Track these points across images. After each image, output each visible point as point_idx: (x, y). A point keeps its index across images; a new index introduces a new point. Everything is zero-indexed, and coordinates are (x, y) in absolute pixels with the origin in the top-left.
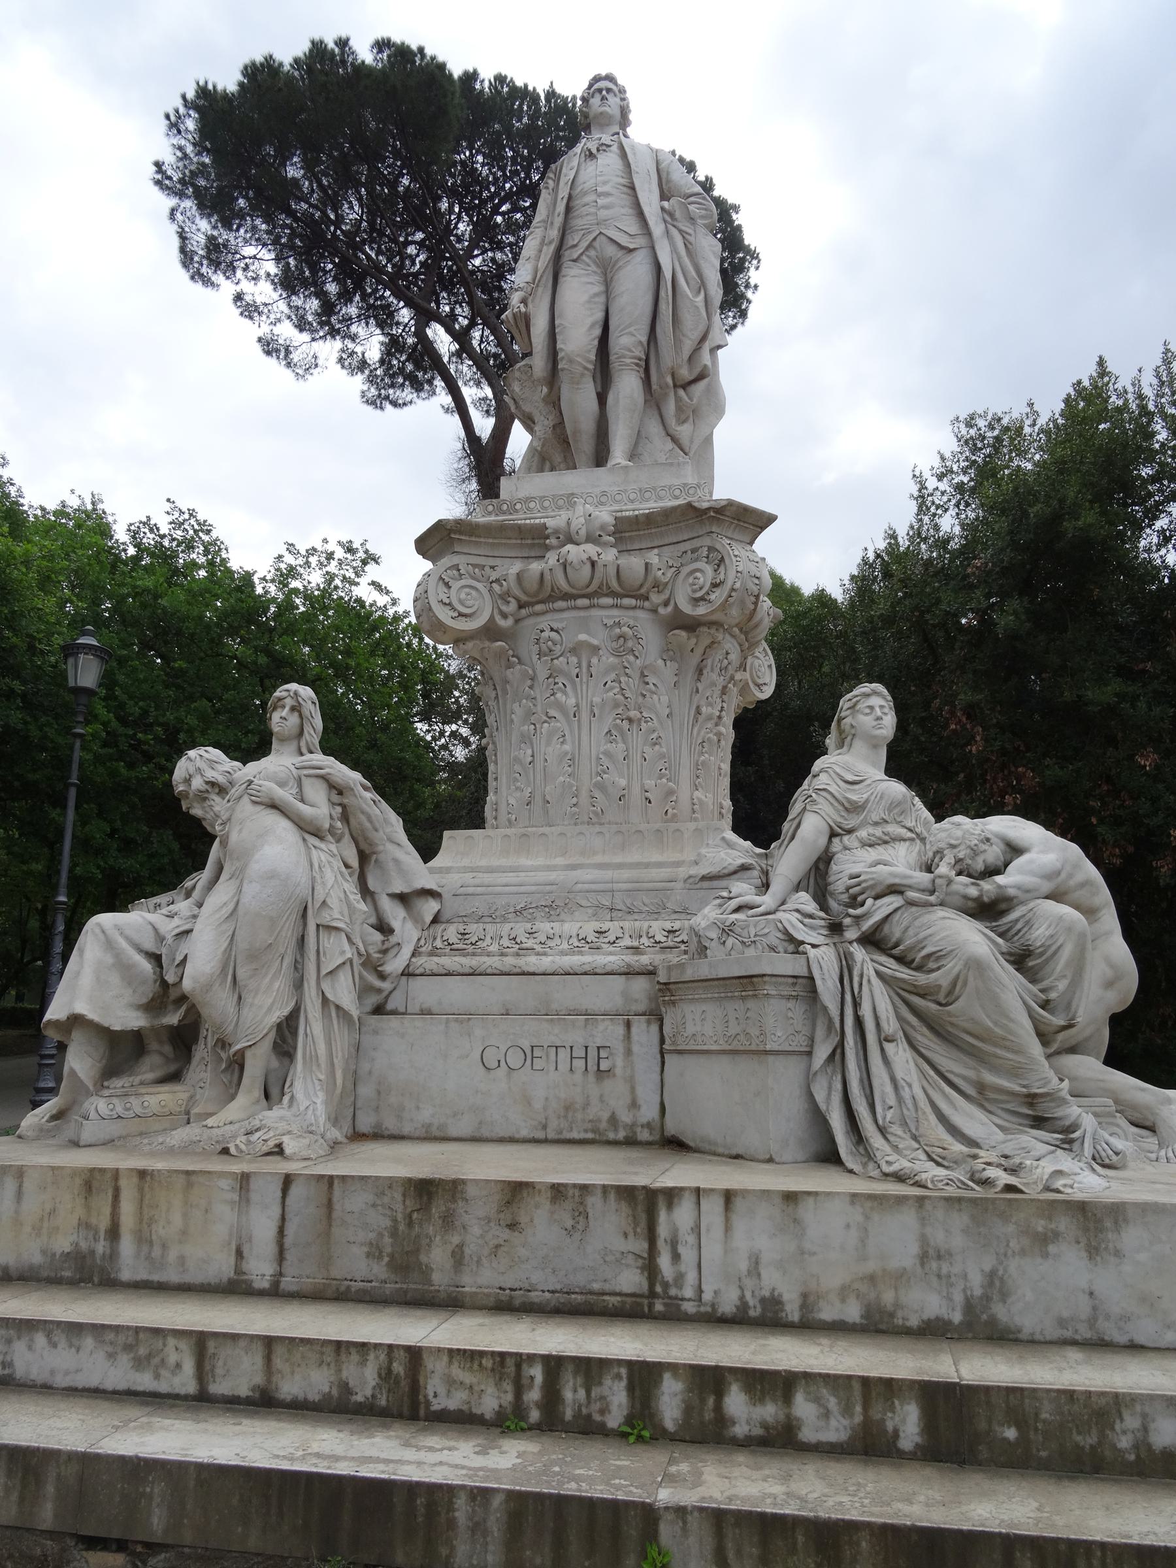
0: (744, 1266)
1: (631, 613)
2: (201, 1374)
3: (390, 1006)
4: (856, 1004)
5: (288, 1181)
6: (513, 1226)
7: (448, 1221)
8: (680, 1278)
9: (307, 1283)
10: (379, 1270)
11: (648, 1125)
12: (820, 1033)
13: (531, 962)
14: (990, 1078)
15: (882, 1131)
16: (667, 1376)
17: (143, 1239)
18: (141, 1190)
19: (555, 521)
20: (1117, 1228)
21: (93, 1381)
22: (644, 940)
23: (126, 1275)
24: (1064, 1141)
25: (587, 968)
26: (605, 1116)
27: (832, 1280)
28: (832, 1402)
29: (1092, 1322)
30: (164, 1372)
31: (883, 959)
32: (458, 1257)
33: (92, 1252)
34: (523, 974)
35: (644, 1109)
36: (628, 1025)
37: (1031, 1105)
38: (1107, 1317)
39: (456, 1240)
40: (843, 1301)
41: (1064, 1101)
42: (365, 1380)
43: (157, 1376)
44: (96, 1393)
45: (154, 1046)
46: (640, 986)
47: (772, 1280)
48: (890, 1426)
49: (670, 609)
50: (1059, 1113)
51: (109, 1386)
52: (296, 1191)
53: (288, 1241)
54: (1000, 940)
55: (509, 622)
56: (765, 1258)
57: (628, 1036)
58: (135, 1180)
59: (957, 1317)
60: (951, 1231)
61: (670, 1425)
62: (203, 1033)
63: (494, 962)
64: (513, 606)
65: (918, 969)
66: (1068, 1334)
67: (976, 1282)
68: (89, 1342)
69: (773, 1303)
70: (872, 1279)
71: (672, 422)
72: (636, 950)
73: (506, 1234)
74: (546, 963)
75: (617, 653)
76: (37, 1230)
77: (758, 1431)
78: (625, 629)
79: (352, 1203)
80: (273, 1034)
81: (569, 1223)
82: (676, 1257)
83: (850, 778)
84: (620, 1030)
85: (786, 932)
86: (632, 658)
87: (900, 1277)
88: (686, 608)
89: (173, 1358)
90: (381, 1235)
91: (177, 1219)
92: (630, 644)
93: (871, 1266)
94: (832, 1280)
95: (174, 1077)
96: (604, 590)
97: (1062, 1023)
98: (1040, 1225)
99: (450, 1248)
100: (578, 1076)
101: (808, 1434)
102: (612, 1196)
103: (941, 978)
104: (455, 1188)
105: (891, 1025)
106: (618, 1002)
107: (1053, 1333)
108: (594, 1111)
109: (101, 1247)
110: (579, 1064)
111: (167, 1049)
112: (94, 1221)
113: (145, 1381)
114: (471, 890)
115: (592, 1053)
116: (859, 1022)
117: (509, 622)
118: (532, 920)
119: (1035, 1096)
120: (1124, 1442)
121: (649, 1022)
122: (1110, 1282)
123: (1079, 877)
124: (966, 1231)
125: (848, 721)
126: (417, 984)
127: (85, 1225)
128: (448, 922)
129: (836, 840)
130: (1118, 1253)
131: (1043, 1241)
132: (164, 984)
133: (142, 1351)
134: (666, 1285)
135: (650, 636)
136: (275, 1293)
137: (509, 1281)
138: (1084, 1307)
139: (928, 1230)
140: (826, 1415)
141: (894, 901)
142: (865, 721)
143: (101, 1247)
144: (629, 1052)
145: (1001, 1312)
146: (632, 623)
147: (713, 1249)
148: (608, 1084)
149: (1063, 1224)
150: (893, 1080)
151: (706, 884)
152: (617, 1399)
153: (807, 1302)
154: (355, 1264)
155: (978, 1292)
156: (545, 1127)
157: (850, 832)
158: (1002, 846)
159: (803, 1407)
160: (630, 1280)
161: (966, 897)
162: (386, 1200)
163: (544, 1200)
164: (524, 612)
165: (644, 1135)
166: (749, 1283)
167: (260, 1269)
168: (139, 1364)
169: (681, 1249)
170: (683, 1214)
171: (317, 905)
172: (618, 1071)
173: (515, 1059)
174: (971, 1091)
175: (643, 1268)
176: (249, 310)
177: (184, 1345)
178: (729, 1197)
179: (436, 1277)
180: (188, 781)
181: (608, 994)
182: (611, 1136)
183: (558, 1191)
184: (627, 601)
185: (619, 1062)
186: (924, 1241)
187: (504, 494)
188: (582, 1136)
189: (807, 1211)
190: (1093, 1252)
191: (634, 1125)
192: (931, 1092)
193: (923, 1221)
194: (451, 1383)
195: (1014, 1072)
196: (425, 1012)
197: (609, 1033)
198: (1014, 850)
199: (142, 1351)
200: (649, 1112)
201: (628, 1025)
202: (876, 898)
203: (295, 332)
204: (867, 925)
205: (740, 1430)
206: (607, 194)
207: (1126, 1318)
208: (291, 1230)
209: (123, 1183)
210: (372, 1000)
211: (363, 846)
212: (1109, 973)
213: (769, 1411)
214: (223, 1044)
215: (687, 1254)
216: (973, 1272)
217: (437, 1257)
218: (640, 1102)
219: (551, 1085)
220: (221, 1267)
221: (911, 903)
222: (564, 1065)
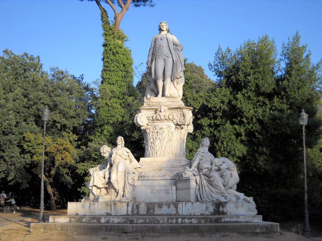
4: (202, 182)
15: (204, 197)
31: (205, 177)
65: (210, 178)
71: (175, 85)
84: (170, 187)
105: (206, 185)
116: (202, 184)
125: (203, 143)
129: (200, 161)
135: (174, 126)
142: (205, 143)
159: (193, 220)
160: (174, 212)
167: (130, 213)
174: (215, 193)
200: (175, 198)
202: (205, 169)
204: (203, 173)
206: (165, 47)
211: (131, 161)
212: (235, 179)
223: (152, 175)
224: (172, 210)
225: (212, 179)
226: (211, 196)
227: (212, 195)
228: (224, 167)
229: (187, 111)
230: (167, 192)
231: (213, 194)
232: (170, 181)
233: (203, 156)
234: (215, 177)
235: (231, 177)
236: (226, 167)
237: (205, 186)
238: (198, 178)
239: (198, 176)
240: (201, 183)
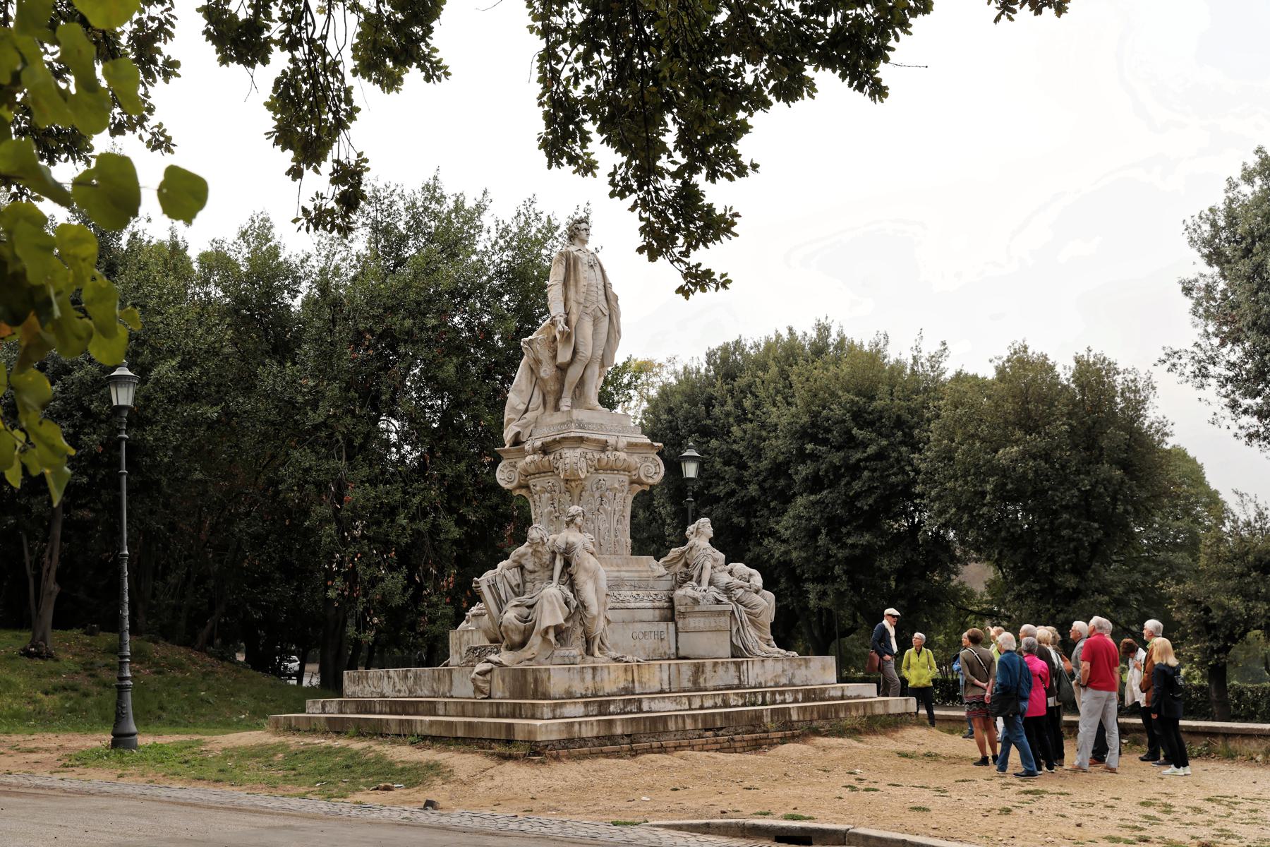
17: (640, 682)
19: (612, 440)
46: (657, 612)
104: (704, 665)
154: (688, 685)
160: (736, 682)
167: (666, 687)
170: (745, 666)
181: (649, 615)
198: (751, 575)
216: (789, 673)
217: (701, 680)
220: (658, 688)
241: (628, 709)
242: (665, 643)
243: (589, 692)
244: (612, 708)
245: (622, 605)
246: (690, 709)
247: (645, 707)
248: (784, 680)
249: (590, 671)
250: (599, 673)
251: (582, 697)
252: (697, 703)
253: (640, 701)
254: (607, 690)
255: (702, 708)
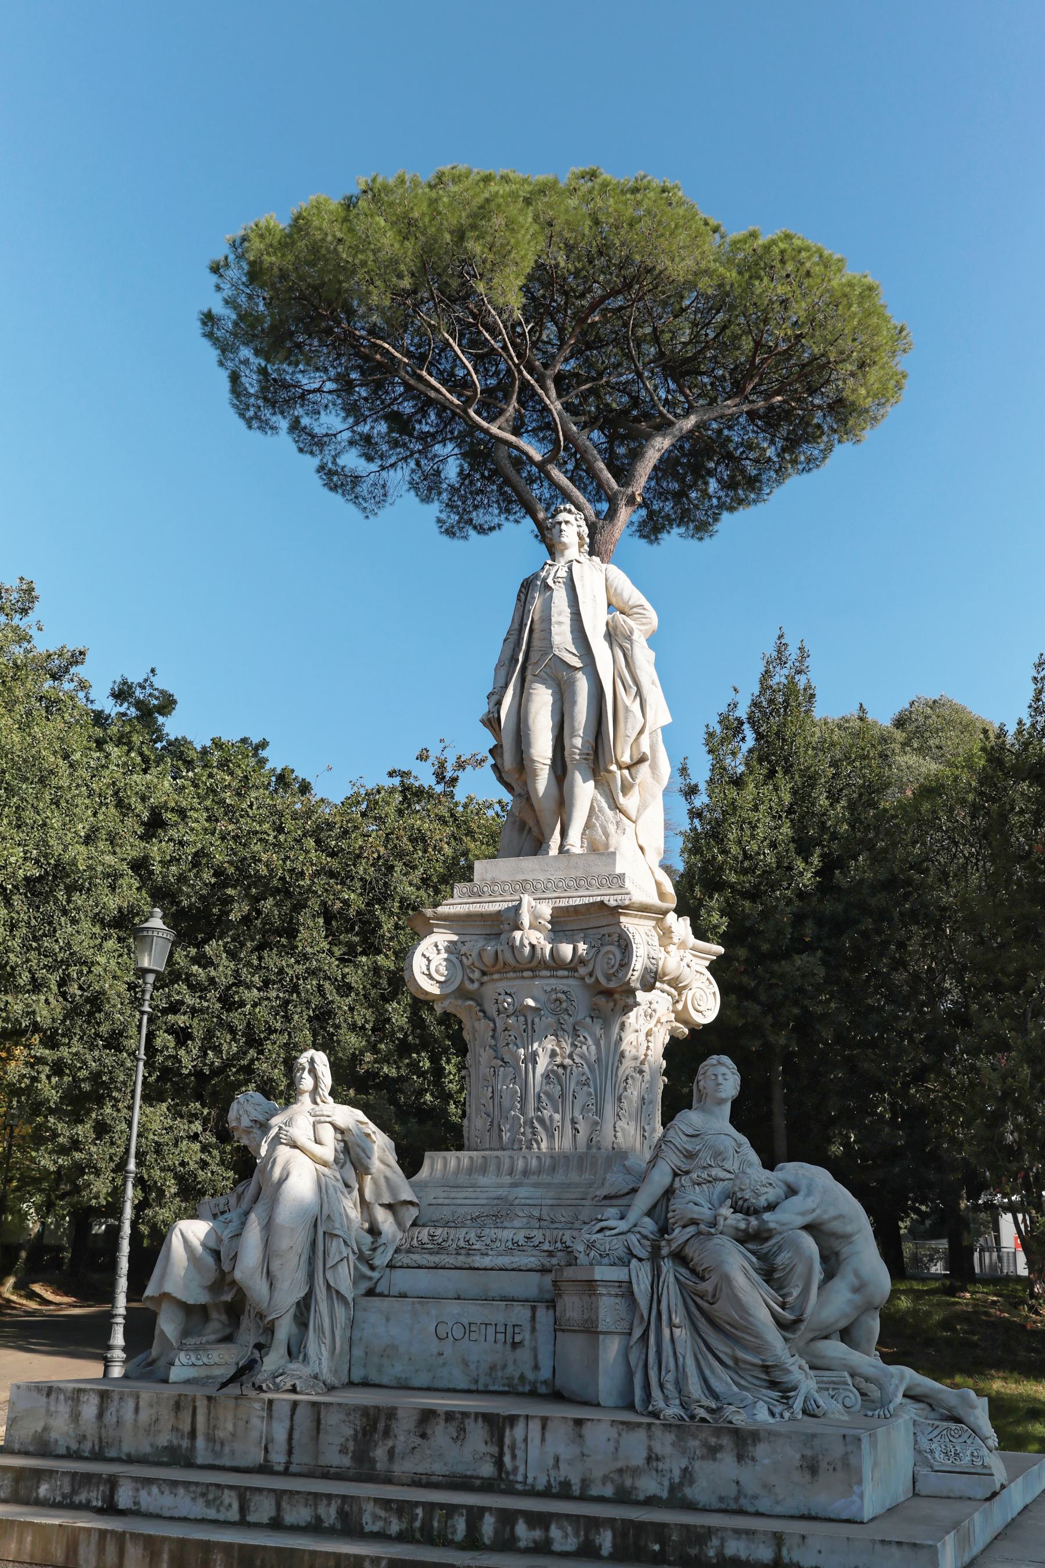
0: (551, 1462)
1: (565, 981)
2: (243, 1510)
3: (378, 1290)
4: (659, 1302)
5: (295, 1404)
6: (423, 1436)
7: (387, 1433)
8: (516, 1469)
9: (304, 1469)
10: (346, 1461)
11: (545, 1382)
12: (636, 1322)
13: (479, 1261)
14: (741, 1354)
15: (661, 1386)
16: (487, 1514)
17: (211, 1439)
18: (209, 1408)
20: (754, 1445)
21: (183, 1513)
22: (559, 1245)
23: (199, 1461)
24: (782, 1397)
25: (514, 1266)
26: (517, 1375)
27: (598, 1473)
28: (569, 1529)
29: (736, 1499)
30: (222, 1509)
31: (683, 1270)
32: (391, 1453)
33: (180, 1446)
34: (471, 1268)
35: (542, 1372)
36: (534, 1309)
37: (767, 1373)
38: (745, 1496)
39: (390, 1443)
40: (604, 1484)
41: (788, 1372)
42: (329, 1514)
43: (218, 1511)
44: (185, 1519)
45: (214, 1315)
47: (565, 1471)
48: (597, 1542)
49: (593, 979)
50: (785, 1379)
51: (192, 1516)
52: (299, 1411)
53: (294, 1443)
54: (754, 1260)
55: (476, 985)
56: (561, 1457)
57: (533, 1318)
58: (205, 1402)
59: (665, 1495)
60: (664, 1443)
61: (487, 1541)
62: (247, 1307)
63: (450, 1260)
64: (477, 975)
66: (723, 1506)
67: (677, 1474)
68: (181, 1491)
69: (566, 1484)
70: (620, 1471)
72: (551, 1254)
73: (419, 1441)
74: (487, 1262)
75: (554, 1013)
76: (148, 1431)
77: (531, 1545)
78: (560, 995)
79: (331, 1419)
80: (292, 1311)
81: (455, 1435)
82: (514, 1457)
83: (690, 1132)
85: (629, 1249)
86: (566, 1017)
87: (635, 1472)
88: (603, 981)
89: (226, 1502)
90: (347, 1440)
91: (230, 1427)
92: (564, 1005)
93: (620, 1464)
94: (598, 1473)
95: (228, 1339)
96: (543, 964)
97: (792, 1317)
98: (713, 1441)
99: (387, 1448)
100: (499, 1346)
101: (557, 1547)
102: (480, 1420)
103: (707, 1286)
104: (391, 1414)
106: (532, 1292)
107: (717, 1505)
108: (510, 1370)
109: (185, 1443)
110: (501, 1337)
111: (224, 1318)
112: (181, 1427)
113: (211, 1514)
114: (440, 1201)
115: (510, 1330)
117: (476, 985)
118: (482, 1227)
119: (767, 1367)
120: (711, 1553)
121: (548, 1308)
122: (749, 1476)
123: (832, 1212)
124: (673, 1444)
126: (398, 1274)
127: (175, 1429)
128: (424, 1226)
129: (677, 1179)
130: (753, 1459)
131: (713, 1452)
132: (222, 1274)
133: (211, 1497)
134: (508, 1473)
136: (286, 1473)
137: (420, 1469)
138: (733, 1491)
139: (652, 1443)
140: (566, 1536)
141: (691, 1230)
143: (185, 1443)
144: (533, 1330)
145: (688, 1491)
146: (566, 989)
147: (534, 1452)
148: (519, 1351)
149: (726, 1441)
150: (675, 1353)
151: (607, 1202)
152: (460, 1525)
153: (585, 1483)
154: (334, 1458)
155: (677, 1480)
156: (476, 1382)
157: (687, 1173)
158: (785, 1188)
159: (555, 1532)
160: (487, 1470)
161: (737, 1229)
162: (352, 1418)
163: (441, 1421)
164: (486, 978)
165: (543, 1390)
166: (553, 1473)
167: (278, 1458)
168: (208, 1504)
169: (517, 1452)
170: (519, 1431)
171: (324, 1218)
172: (526, 1343)
173: (458, 1333)
174: (730, 1362)
175: (495, 1463)
176: (311, 442)
177: (233, 1494)
178: (527, 1417)
179: (378, 1466)
180: (239, 1120)
182: (520, 1389)
183: (450, 1416)
184: (561, 973)
185: (527, 1336)
186: (650, 1448)
187: (477, 876)
188: (501, 1389)
189: (587, 1430)
190: (740, 1458)
191: (535, 1382)
192: (702, 1362)
193: (650, 1437)
194: (376, 1518)
195: (756, 1350)
196: (403, 1296)
197: (521, 1314)
199: (211, 1497)
200: (545, 1373)
201: (534, 1309)
202: (684, 1227)
203: (362, 462)
204: (674, 1246)
205: (522, 1544)
207: (755, 1497)
208: (296, 1435)
209: (198, 1404)
210: (364, 1286)
213: (537, 1534)
214: (261, 1316)
215: (519, 1453)
217: (380, 1453)
218: (541, 1365)
219: (483, 1351)
220: (257, 1457)
221: (699, 1233)
222: (491, 1338)
223: (462, 1244)
224: (473, 1453)
225: (707, 1286)
226: (705, 1380)
227: (707, 1372)
228: (788, 1217)
229: (636, 921)
230: (509, 1340)
231: (713, 1372)
232: (536, 1276)
233: (690, 1156)
234: (727, 1279)
235: (830, 1275)
236: (802, 1221)
237: (671, 1325)
238: (641, 1276)
239: (647, 1267)
240: (655, 1306)
241: (82, 1497)
242: (524, 1355)
243: (87, 1446)
244: (43, 1490)
245: (461, 1260)
246: (243, 1523)
247: (124, 1498)
248: (649, 1485)
249: (95, 1400)
250: (112, 1408)
251: (71, 1455)
252: (263, 1510)
253: (112, 1483)
254: (128, 1447)
255: (276, 1525)
